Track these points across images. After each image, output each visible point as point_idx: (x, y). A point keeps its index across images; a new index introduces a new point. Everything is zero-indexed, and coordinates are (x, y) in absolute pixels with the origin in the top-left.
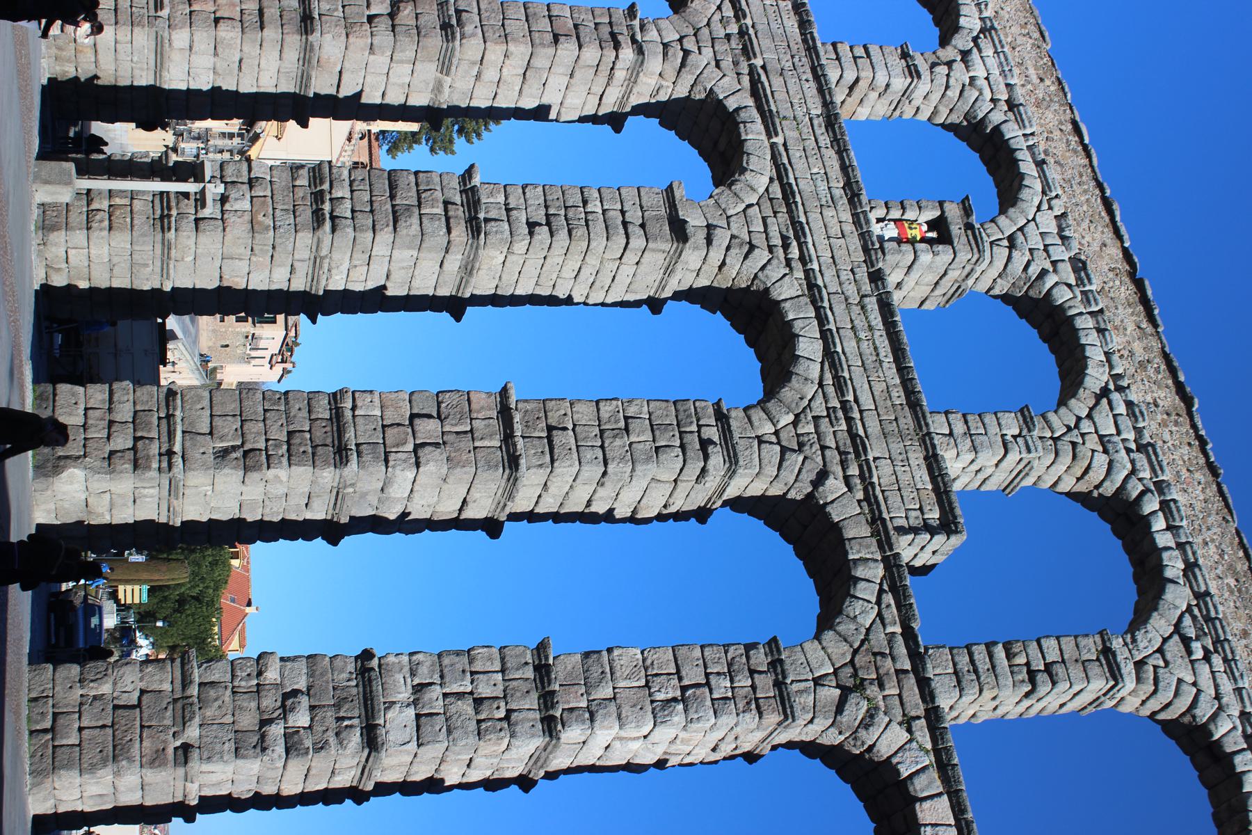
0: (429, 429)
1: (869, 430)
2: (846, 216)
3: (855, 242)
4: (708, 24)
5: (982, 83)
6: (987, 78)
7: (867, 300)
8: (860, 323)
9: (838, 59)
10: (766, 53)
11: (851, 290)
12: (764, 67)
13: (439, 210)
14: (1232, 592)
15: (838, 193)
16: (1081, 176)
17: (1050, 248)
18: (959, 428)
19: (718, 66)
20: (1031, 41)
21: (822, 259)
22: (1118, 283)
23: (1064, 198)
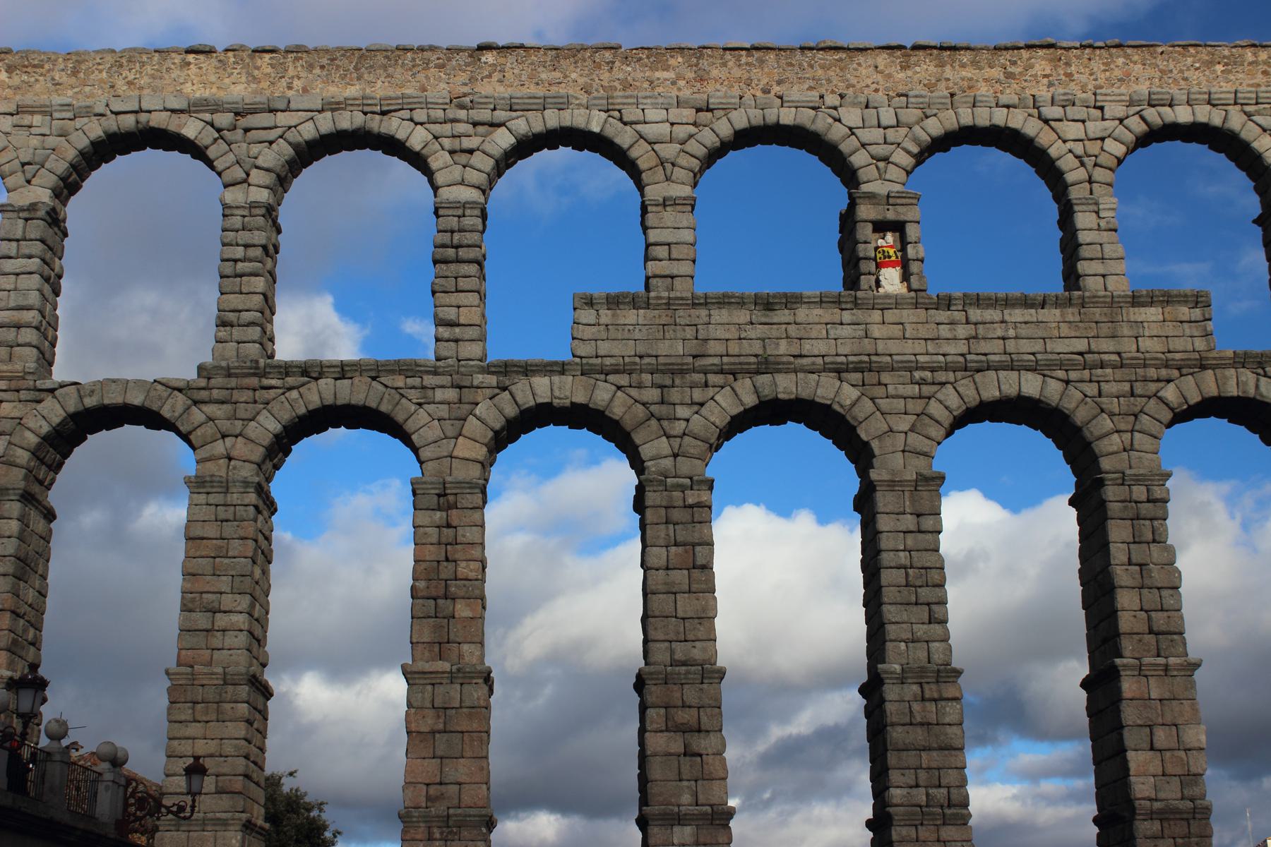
0: (1161, 736)
1: (1111, 349)
2: (876, 315)
3: (908, 315)
4: (643, 404)
5: (681, 131)
6: (672, 124)
7: (973, 318)
8: (999, 333)
9: (672, 277)
10: (673, 348)
11: (962, 331)
12: (694, 357)
13: (931, 707)
14: (1230, 72)
15: (847, 316)
16: (791, 65)
17: (884, 122)
18: (1096, 267)
19: (702, 405)
20: (617, 64)
21: (931, 349)
22: (918, 69)
23: (824, 91)
